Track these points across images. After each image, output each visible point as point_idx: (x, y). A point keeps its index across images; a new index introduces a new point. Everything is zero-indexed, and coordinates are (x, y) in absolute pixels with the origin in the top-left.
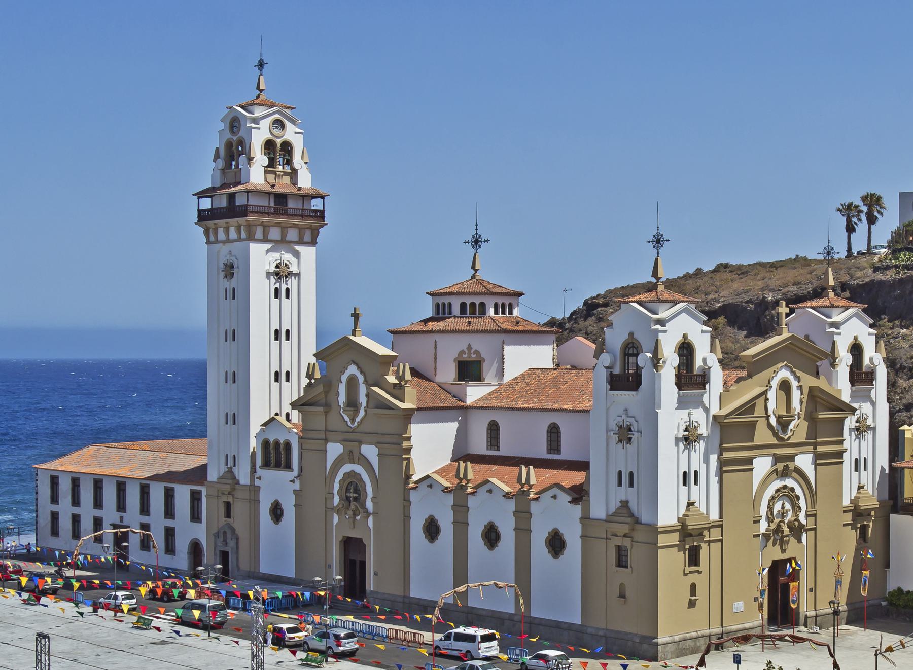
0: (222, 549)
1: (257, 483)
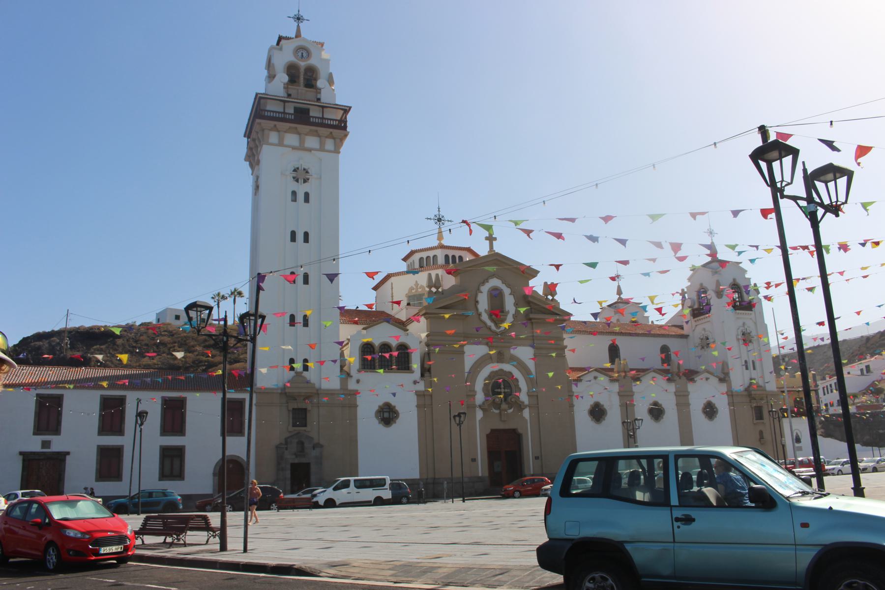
0: (296, 461)
1: (352, 385)
